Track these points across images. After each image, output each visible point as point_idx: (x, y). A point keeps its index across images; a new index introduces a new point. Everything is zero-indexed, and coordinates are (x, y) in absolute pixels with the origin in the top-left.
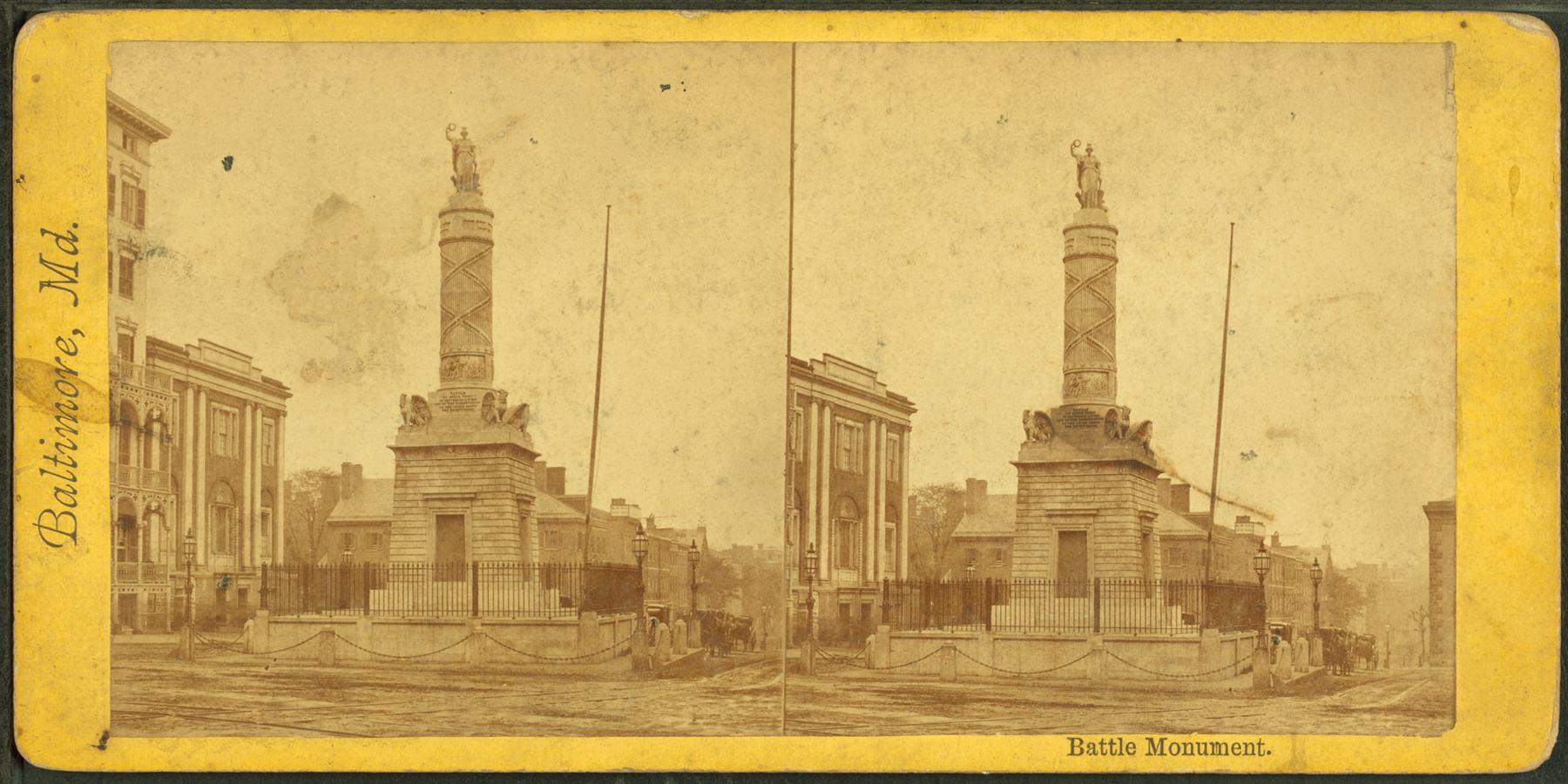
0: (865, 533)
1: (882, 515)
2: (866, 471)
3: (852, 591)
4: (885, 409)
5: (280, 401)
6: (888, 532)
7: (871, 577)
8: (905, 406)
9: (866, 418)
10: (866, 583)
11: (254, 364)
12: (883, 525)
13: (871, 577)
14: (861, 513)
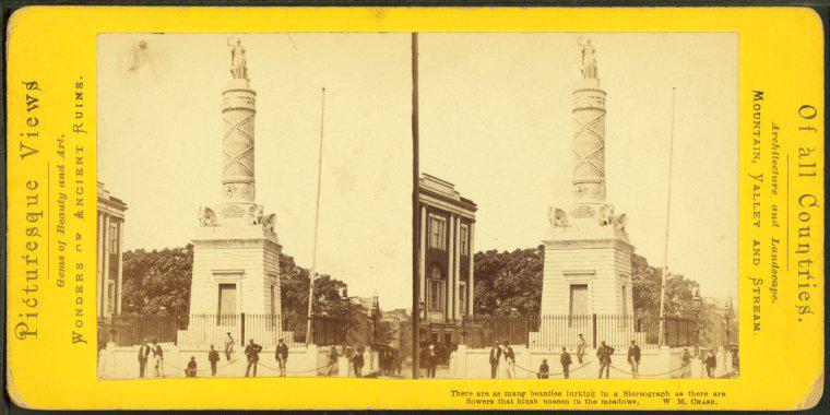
0: (447, 285)
1: (458, 277)
2: (448, 251)
3: (438, 325)
4: (459, 209)
5: (121, 213)
6: (461, 287)
7: (450, 316)
8: (470, 205)
9: (447, 214)
10: (447, 320)
11: (105, 187)
12: (458, 283)
13: (450, 316)
14: (445, 275)
